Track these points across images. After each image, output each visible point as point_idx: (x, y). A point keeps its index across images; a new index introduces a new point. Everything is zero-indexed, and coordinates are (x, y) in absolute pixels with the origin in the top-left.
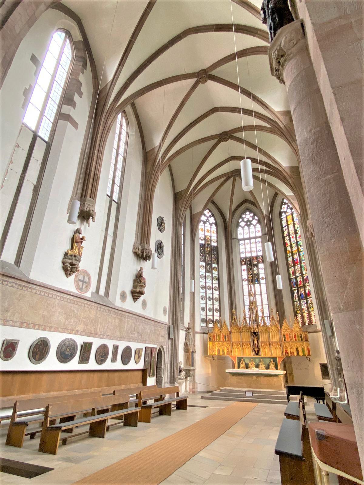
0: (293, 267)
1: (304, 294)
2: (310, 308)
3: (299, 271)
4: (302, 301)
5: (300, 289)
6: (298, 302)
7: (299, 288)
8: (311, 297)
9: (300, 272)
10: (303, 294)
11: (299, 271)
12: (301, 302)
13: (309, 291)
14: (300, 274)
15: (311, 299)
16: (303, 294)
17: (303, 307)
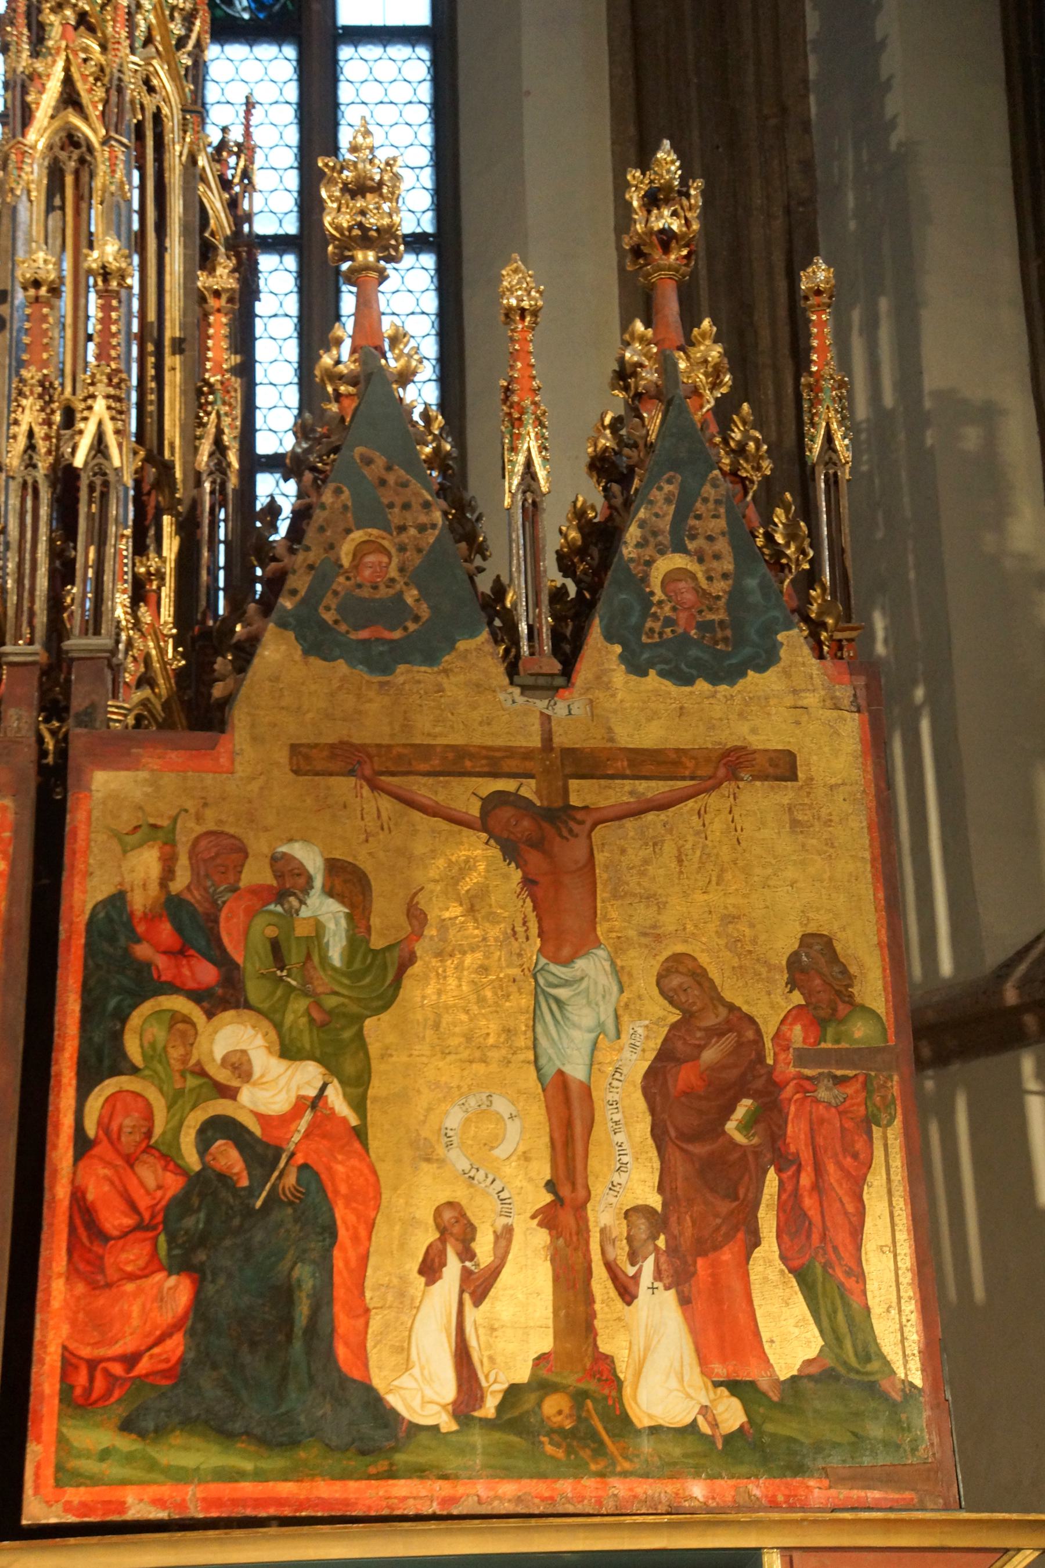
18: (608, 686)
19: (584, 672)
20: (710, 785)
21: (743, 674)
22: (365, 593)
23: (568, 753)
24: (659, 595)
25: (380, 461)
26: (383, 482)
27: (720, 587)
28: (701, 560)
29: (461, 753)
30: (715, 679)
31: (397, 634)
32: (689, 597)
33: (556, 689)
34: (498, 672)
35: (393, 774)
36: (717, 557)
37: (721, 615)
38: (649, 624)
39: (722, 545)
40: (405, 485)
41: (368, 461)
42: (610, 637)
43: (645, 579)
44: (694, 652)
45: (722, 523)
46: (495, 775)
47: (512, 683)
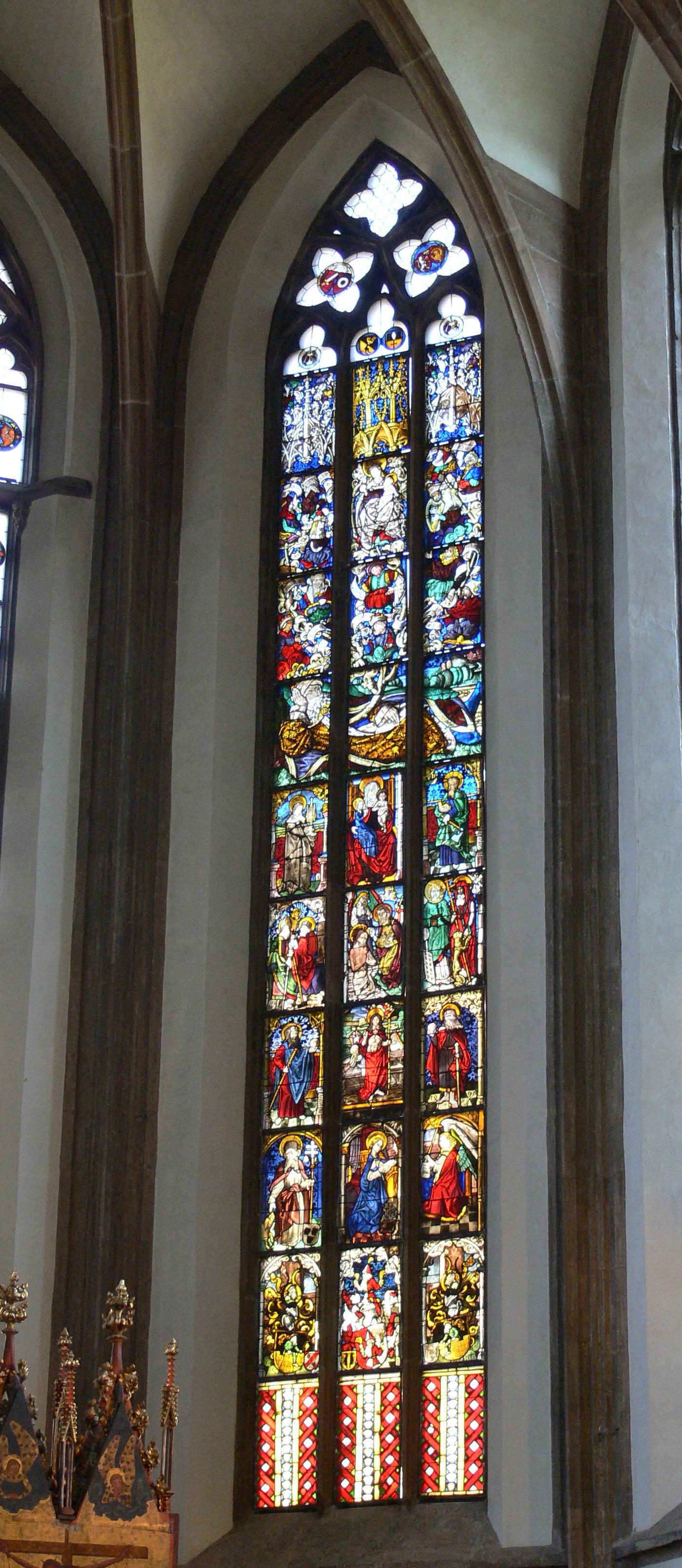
0: (317, 904)
1: (393, 1190)
2: (438, 1334)
3: (378, 953)
4: (352, 1255)
5: (362, 1137)
6: (311, 1262)
7: (350, 1120)
8: (464, 1232)
9: (387, 962)
10: (381, 1183)
11: (378, 953)
12: (347, 1271)
13: (452, 1167)
14: (389, 980)
15: (472, 1245)
16: (381, 1183)
17: (349, 1319)
18: (88, 1520)
19: (82, 1513)
20: (119, 1559)
21: (134, 1517)
22: (10, 1480)
23: (75, 1546)
24: (109, 1484)
25: (19, 1427)
26: (19, 1436)
27: (130, 1482)
28: (124, 1471)
29: (38, 1544)
30: (124, 1520)
31: (20, 1497)
32: (119, 1485)
33: (71, 1521)
34: (52, 1511)
35: (14, 1551)
36: (130, 1470)
37: (128, 1493)
38: (105, 1496)
39: (132, 1466)
40: (27, 1437)
41: (15, 1427)
42: (91, 1500)
43: (105, 1479)
44: (118, 1508)
45: (132, 1457)
46: (49, 1553)
47: (57, 1518)
